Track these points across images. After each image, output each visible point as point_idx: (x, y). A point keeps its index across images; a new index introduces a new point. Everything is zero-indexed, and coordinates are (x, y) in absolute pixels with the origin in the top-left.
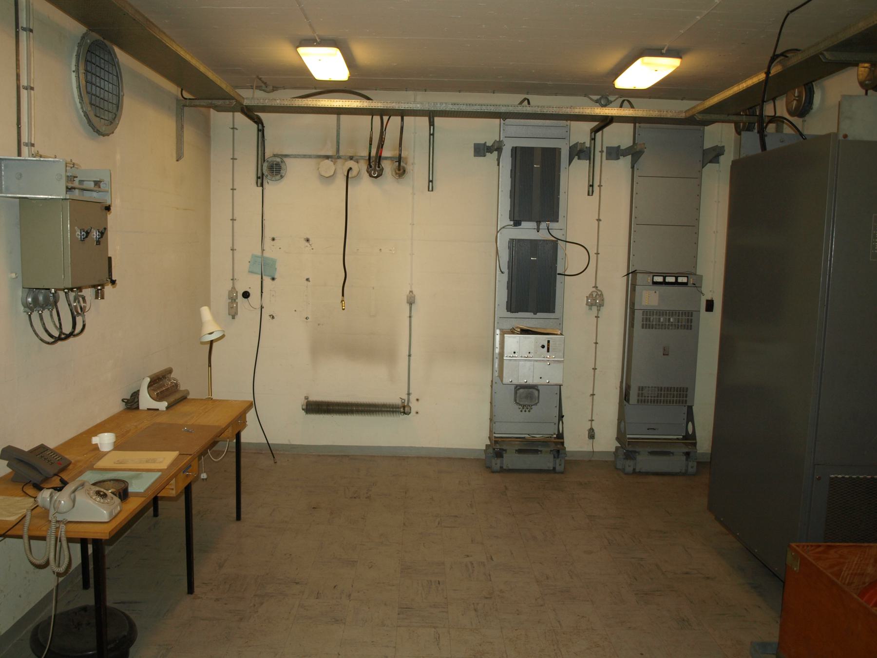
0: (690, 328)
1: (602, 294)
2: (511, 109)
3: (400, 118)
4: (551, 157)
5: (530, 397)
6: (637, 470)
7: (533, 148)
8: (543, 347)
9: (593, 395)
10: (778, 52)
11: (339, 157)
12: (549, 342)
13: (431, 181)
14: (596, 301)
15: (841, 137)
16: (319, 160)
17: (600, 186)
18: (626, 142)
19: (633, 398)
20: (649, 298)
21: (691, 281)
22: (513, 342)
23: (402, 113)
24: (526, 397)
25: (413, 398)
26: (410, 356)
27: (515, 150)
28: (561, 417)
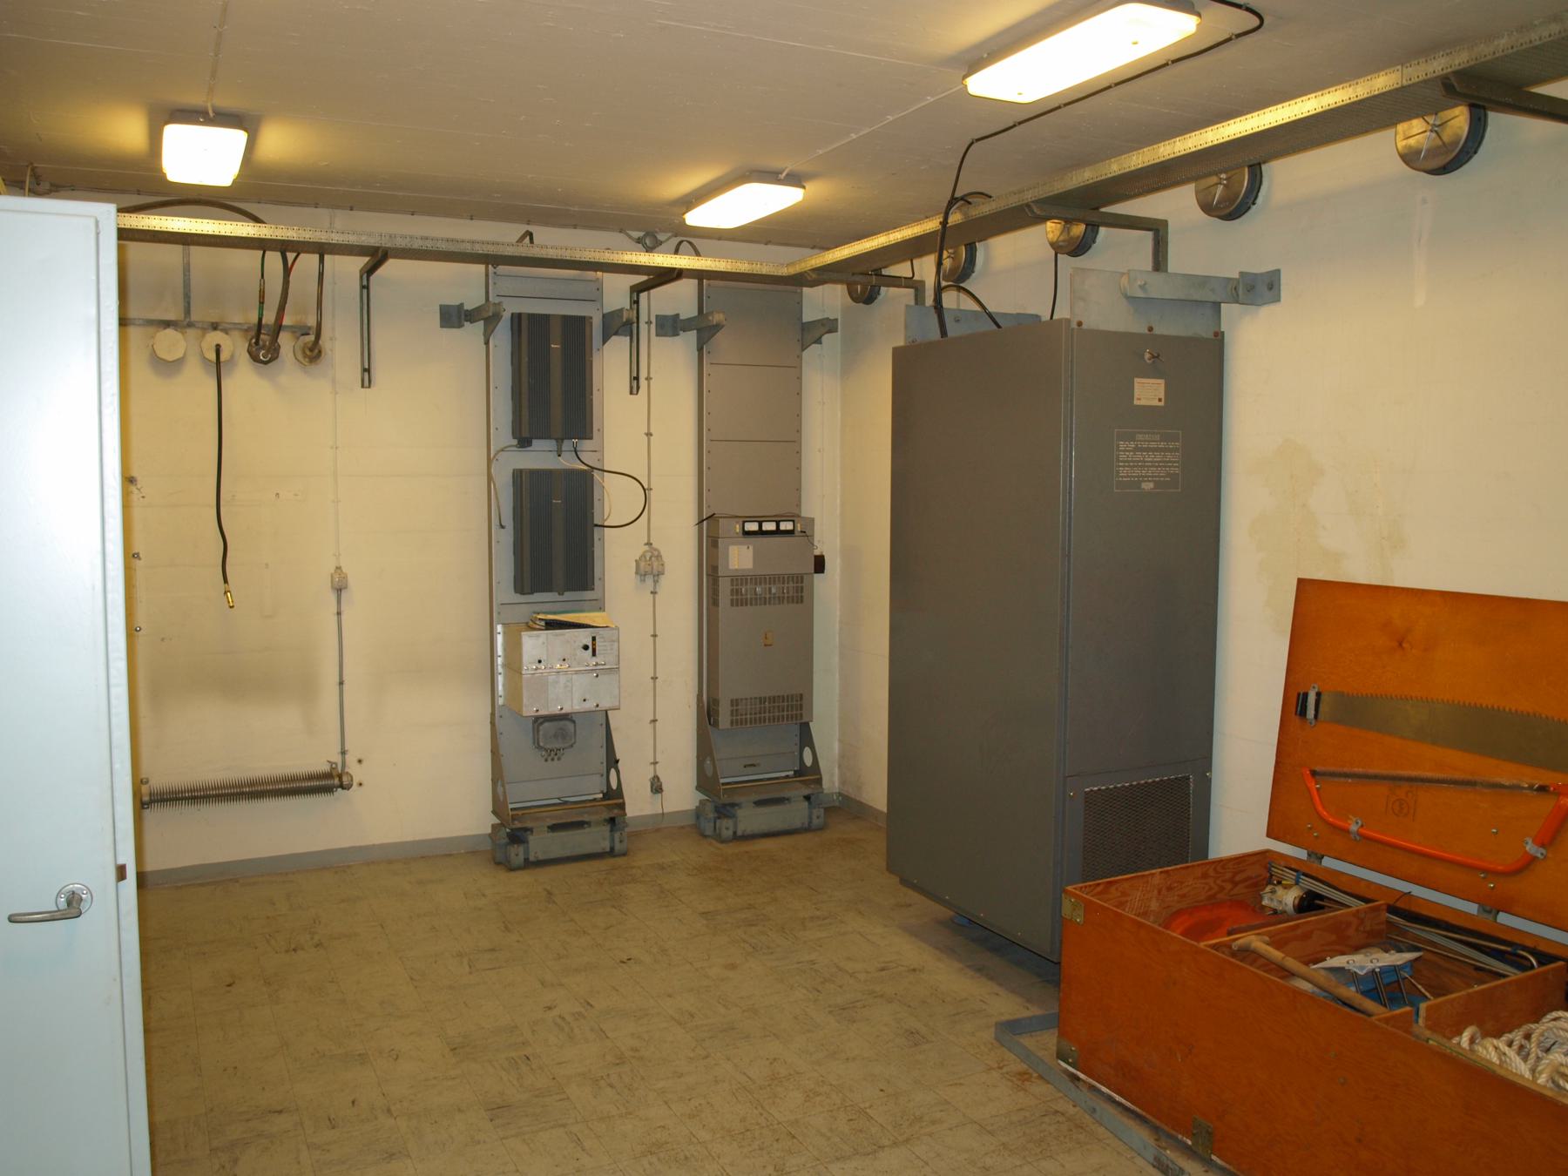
0: (800, 600)
1: (659, 557)
2: (510, 251)
3: (316, 257)
4: (576, 329)
5: (562, 735)
6: (739, 833)
7: (547, 317)
8: (586, 648)
9: (654, 721)
10: (958, 195)
11: (190, 325)
12: (594, 639)
13: (367, 371)
14: (650, 569)
15: (1074, 325)
16: (151, 330)
17: (648, 379)
18: (688, 310)
19: (724, 719)
20: (740, 557)
21: (799, 528)
22: (534, 645)
23: (322, 250)
24: (555, 736)
25: (351, 759)
26: (341, 683)
27: (517, 319)
28: (612, 762)
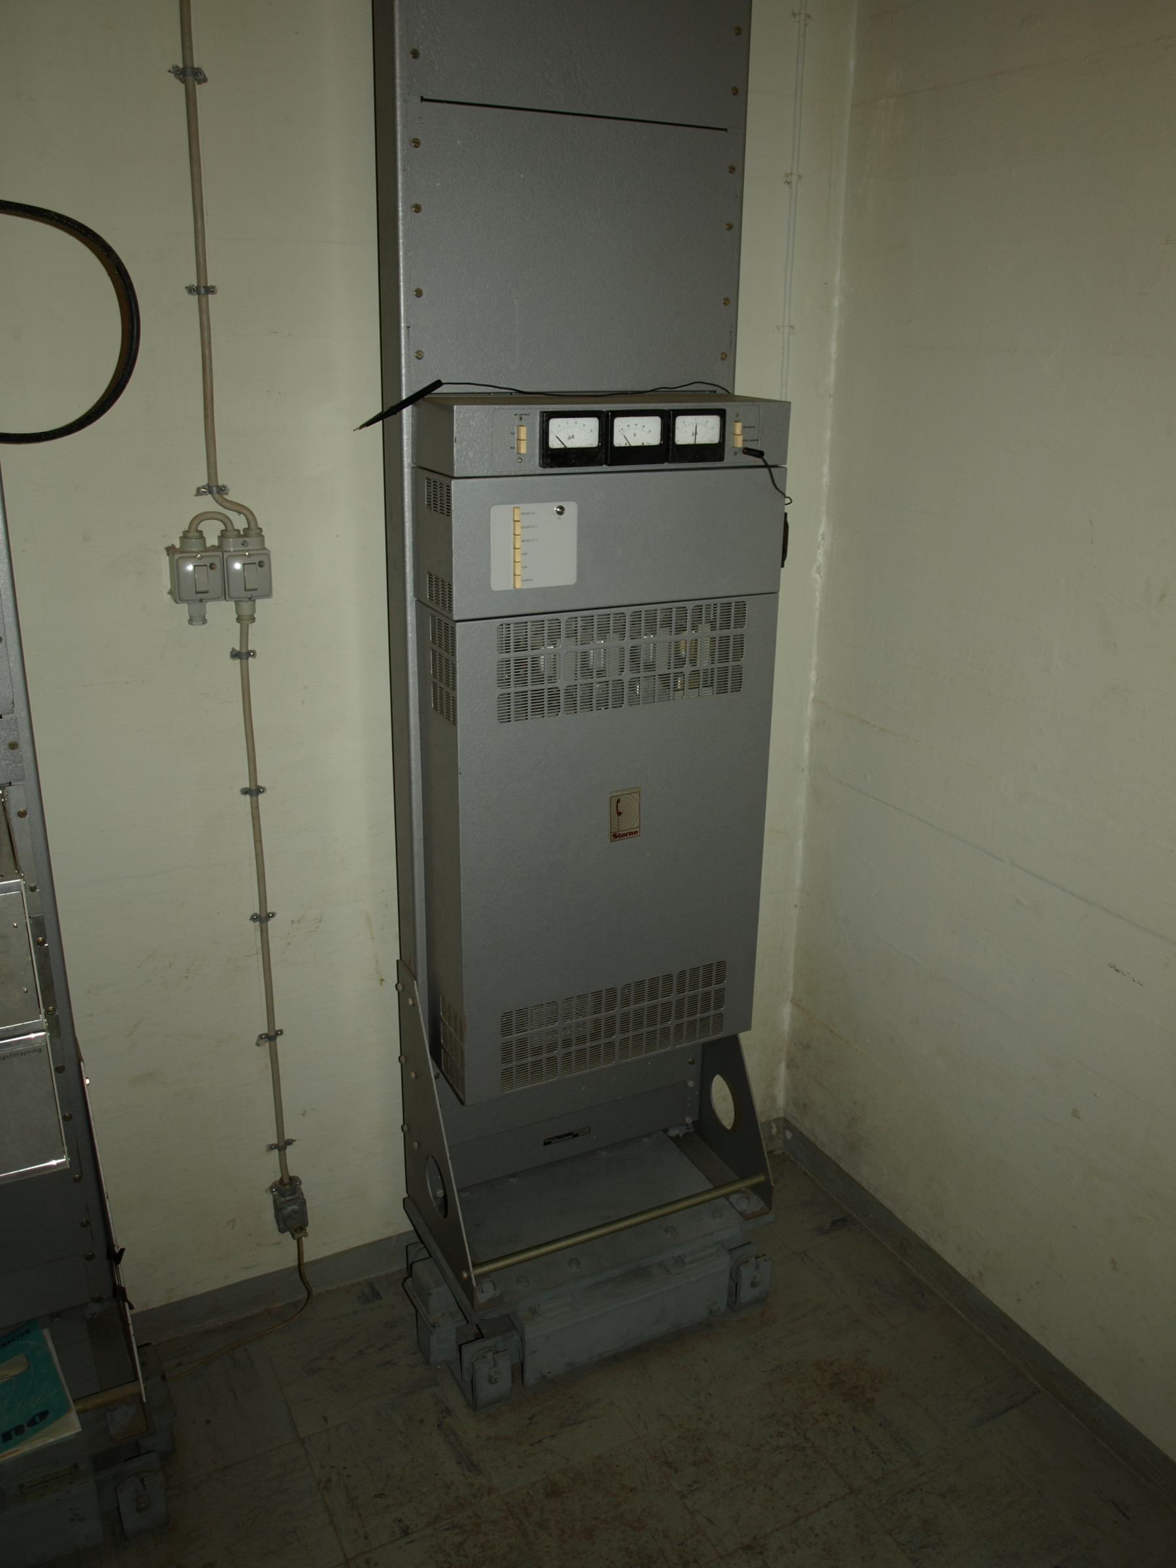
0: (727, 680)
1: (253, 531)
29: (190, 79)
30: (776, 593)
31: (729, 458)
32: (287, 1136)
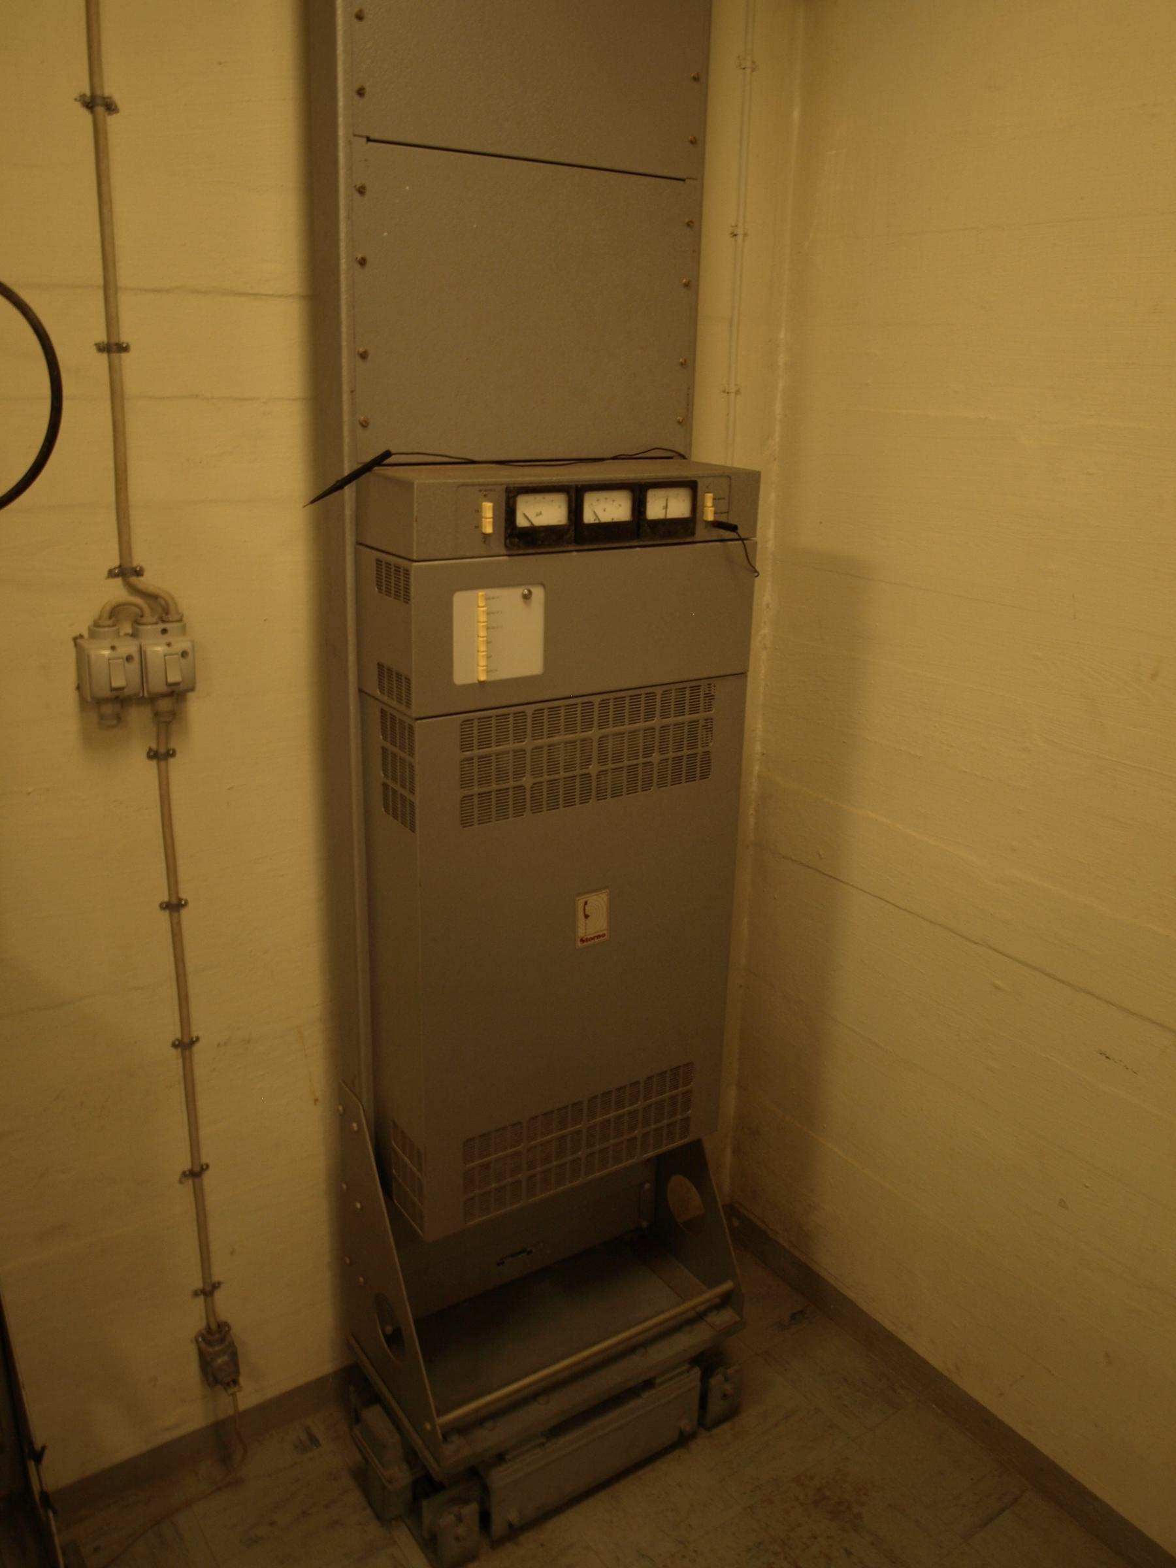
9: (195, 1173)
20: (496, 634)
29: (100, 110)
30: (743, 675)
31: (701, 532)
32: (216, 1278)
